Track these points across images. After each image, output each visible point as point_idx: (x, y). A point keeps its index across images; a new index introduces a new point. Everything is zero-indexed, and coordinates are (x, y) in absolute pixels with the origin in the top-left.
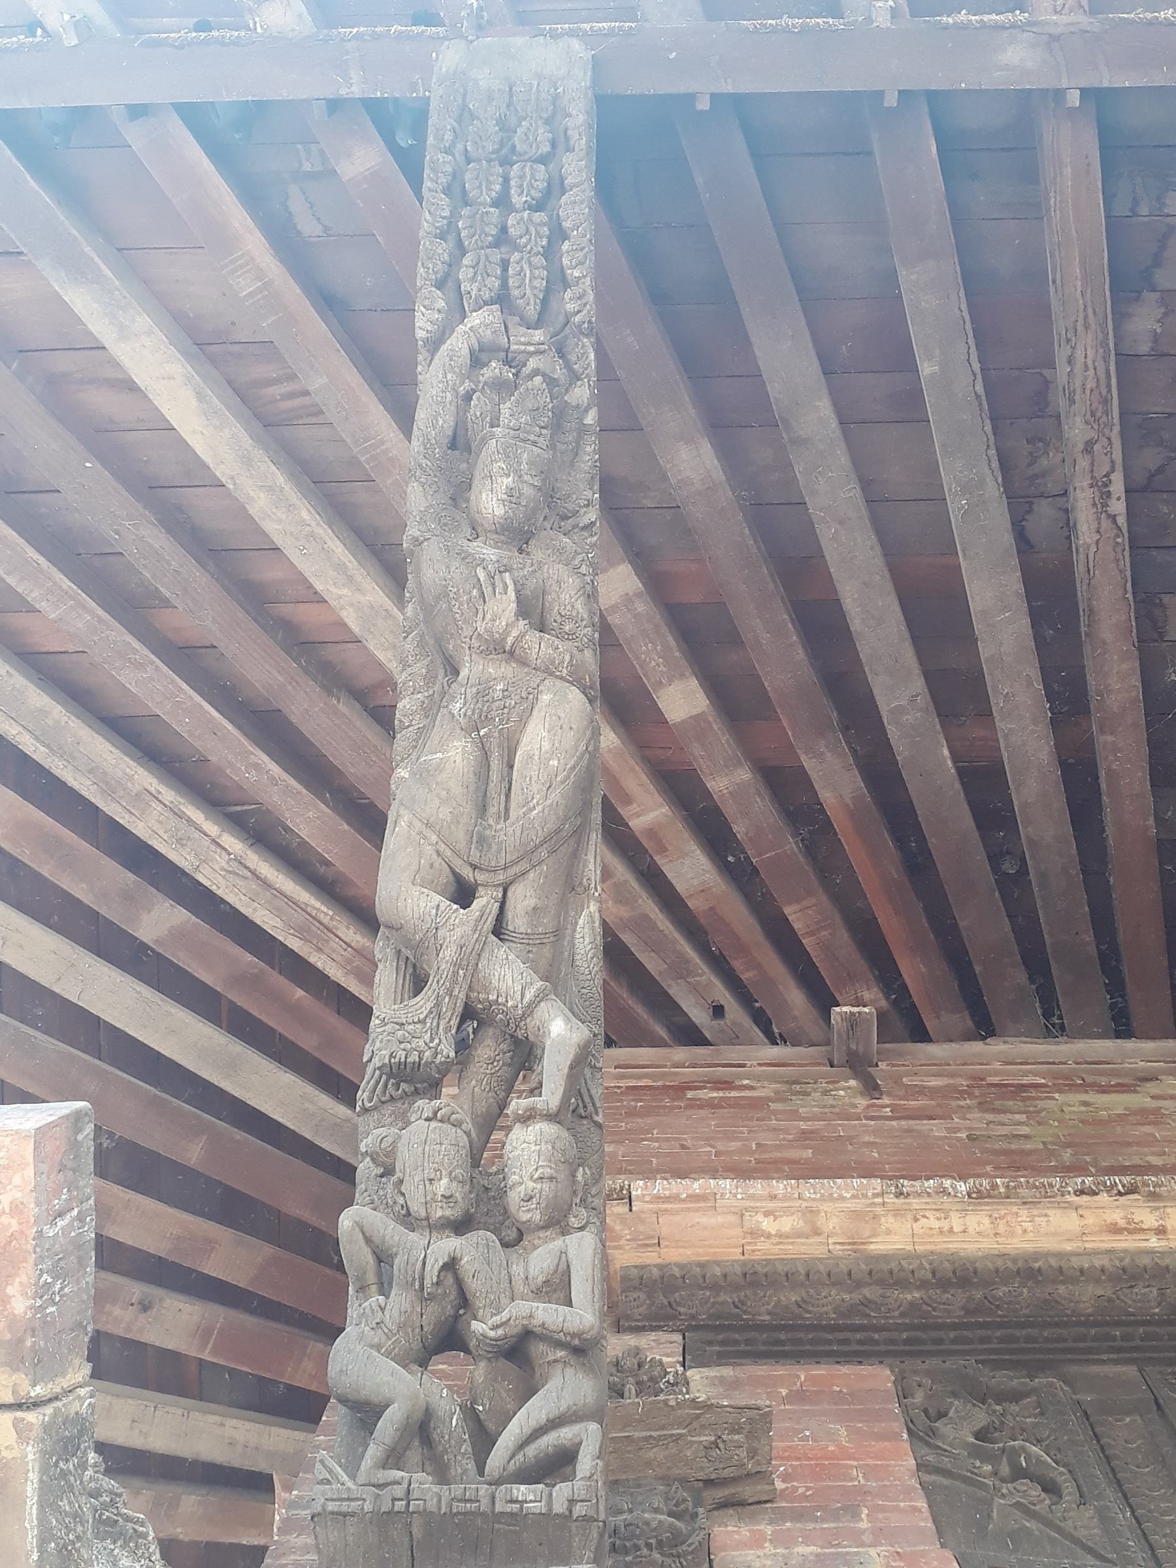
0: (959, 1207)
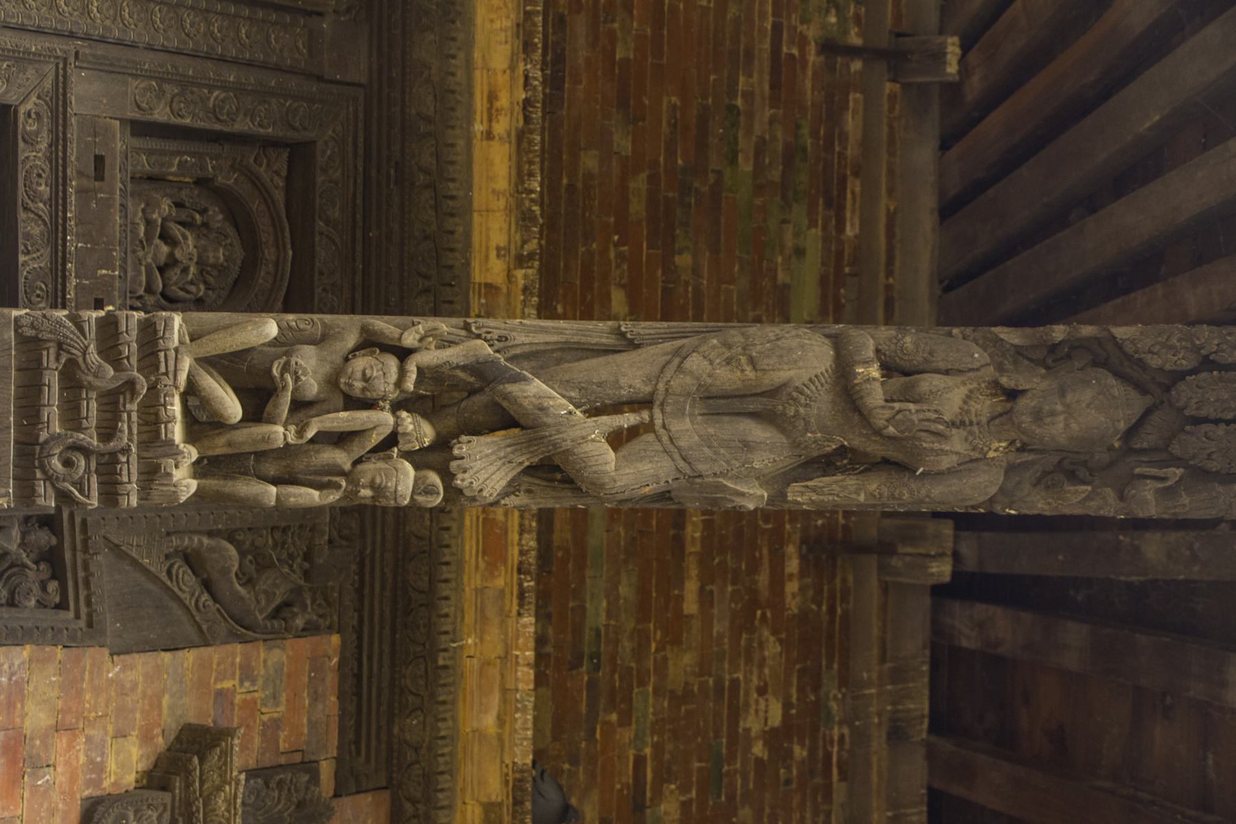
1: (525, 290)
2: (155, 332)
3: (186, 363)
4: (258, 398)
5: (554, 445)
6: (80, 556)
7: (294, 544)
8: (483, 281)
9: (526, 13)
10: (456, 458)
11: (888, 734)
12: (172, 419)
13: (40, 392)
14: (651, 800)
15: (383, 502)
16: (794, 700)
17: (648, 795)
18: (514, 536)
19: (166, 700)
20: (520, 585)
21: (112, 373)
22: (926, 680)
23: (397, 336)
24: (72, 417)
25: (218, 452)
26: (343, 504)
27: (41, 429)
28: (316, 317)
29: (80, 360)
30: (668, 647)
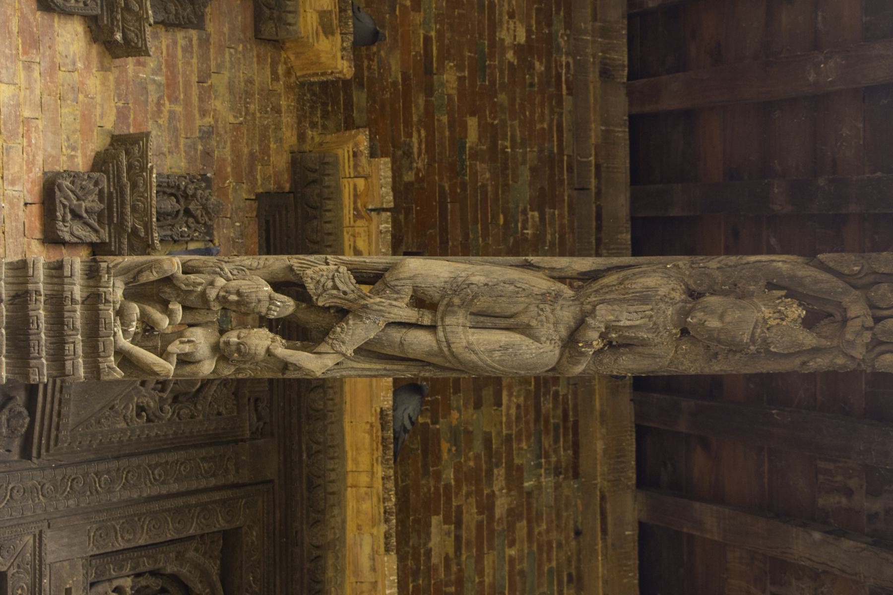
11: (600, 72)
14: (437, 69)
17: (435, 65)
22: (625, 40)
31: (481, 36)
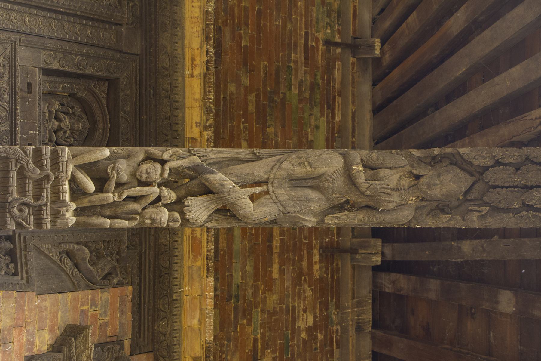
0: (203, 6)
1: (208, 140)
2: (58, 154)
3: (71, 167)
4: (101, 182)
5: (228, 200)
6: (23, 252)
7: (112, 248)
8: (190, 137)
9: (206, 24)
10: (186, 206)
12: (65, 191)
13: (9, 180)
14: (261, 357)
15: (156, 225)
16: (318, 315)
17: (259, 355)
18: (204, 244)
19: (60, 314)
20: (207, 265)
21: (39, 172)
23: (160, 155)
24: (22, 191)
25: (85, 205)
26: (138, 227)
27: (9, 196)
28: (125, 148)
29: (26, 166)
30: (267, 292)
31: (287, 330)
